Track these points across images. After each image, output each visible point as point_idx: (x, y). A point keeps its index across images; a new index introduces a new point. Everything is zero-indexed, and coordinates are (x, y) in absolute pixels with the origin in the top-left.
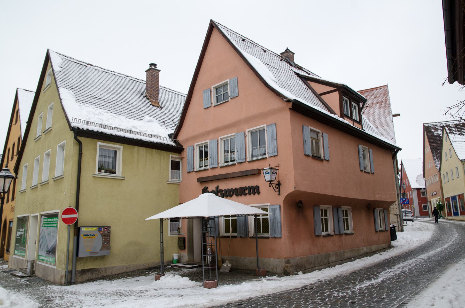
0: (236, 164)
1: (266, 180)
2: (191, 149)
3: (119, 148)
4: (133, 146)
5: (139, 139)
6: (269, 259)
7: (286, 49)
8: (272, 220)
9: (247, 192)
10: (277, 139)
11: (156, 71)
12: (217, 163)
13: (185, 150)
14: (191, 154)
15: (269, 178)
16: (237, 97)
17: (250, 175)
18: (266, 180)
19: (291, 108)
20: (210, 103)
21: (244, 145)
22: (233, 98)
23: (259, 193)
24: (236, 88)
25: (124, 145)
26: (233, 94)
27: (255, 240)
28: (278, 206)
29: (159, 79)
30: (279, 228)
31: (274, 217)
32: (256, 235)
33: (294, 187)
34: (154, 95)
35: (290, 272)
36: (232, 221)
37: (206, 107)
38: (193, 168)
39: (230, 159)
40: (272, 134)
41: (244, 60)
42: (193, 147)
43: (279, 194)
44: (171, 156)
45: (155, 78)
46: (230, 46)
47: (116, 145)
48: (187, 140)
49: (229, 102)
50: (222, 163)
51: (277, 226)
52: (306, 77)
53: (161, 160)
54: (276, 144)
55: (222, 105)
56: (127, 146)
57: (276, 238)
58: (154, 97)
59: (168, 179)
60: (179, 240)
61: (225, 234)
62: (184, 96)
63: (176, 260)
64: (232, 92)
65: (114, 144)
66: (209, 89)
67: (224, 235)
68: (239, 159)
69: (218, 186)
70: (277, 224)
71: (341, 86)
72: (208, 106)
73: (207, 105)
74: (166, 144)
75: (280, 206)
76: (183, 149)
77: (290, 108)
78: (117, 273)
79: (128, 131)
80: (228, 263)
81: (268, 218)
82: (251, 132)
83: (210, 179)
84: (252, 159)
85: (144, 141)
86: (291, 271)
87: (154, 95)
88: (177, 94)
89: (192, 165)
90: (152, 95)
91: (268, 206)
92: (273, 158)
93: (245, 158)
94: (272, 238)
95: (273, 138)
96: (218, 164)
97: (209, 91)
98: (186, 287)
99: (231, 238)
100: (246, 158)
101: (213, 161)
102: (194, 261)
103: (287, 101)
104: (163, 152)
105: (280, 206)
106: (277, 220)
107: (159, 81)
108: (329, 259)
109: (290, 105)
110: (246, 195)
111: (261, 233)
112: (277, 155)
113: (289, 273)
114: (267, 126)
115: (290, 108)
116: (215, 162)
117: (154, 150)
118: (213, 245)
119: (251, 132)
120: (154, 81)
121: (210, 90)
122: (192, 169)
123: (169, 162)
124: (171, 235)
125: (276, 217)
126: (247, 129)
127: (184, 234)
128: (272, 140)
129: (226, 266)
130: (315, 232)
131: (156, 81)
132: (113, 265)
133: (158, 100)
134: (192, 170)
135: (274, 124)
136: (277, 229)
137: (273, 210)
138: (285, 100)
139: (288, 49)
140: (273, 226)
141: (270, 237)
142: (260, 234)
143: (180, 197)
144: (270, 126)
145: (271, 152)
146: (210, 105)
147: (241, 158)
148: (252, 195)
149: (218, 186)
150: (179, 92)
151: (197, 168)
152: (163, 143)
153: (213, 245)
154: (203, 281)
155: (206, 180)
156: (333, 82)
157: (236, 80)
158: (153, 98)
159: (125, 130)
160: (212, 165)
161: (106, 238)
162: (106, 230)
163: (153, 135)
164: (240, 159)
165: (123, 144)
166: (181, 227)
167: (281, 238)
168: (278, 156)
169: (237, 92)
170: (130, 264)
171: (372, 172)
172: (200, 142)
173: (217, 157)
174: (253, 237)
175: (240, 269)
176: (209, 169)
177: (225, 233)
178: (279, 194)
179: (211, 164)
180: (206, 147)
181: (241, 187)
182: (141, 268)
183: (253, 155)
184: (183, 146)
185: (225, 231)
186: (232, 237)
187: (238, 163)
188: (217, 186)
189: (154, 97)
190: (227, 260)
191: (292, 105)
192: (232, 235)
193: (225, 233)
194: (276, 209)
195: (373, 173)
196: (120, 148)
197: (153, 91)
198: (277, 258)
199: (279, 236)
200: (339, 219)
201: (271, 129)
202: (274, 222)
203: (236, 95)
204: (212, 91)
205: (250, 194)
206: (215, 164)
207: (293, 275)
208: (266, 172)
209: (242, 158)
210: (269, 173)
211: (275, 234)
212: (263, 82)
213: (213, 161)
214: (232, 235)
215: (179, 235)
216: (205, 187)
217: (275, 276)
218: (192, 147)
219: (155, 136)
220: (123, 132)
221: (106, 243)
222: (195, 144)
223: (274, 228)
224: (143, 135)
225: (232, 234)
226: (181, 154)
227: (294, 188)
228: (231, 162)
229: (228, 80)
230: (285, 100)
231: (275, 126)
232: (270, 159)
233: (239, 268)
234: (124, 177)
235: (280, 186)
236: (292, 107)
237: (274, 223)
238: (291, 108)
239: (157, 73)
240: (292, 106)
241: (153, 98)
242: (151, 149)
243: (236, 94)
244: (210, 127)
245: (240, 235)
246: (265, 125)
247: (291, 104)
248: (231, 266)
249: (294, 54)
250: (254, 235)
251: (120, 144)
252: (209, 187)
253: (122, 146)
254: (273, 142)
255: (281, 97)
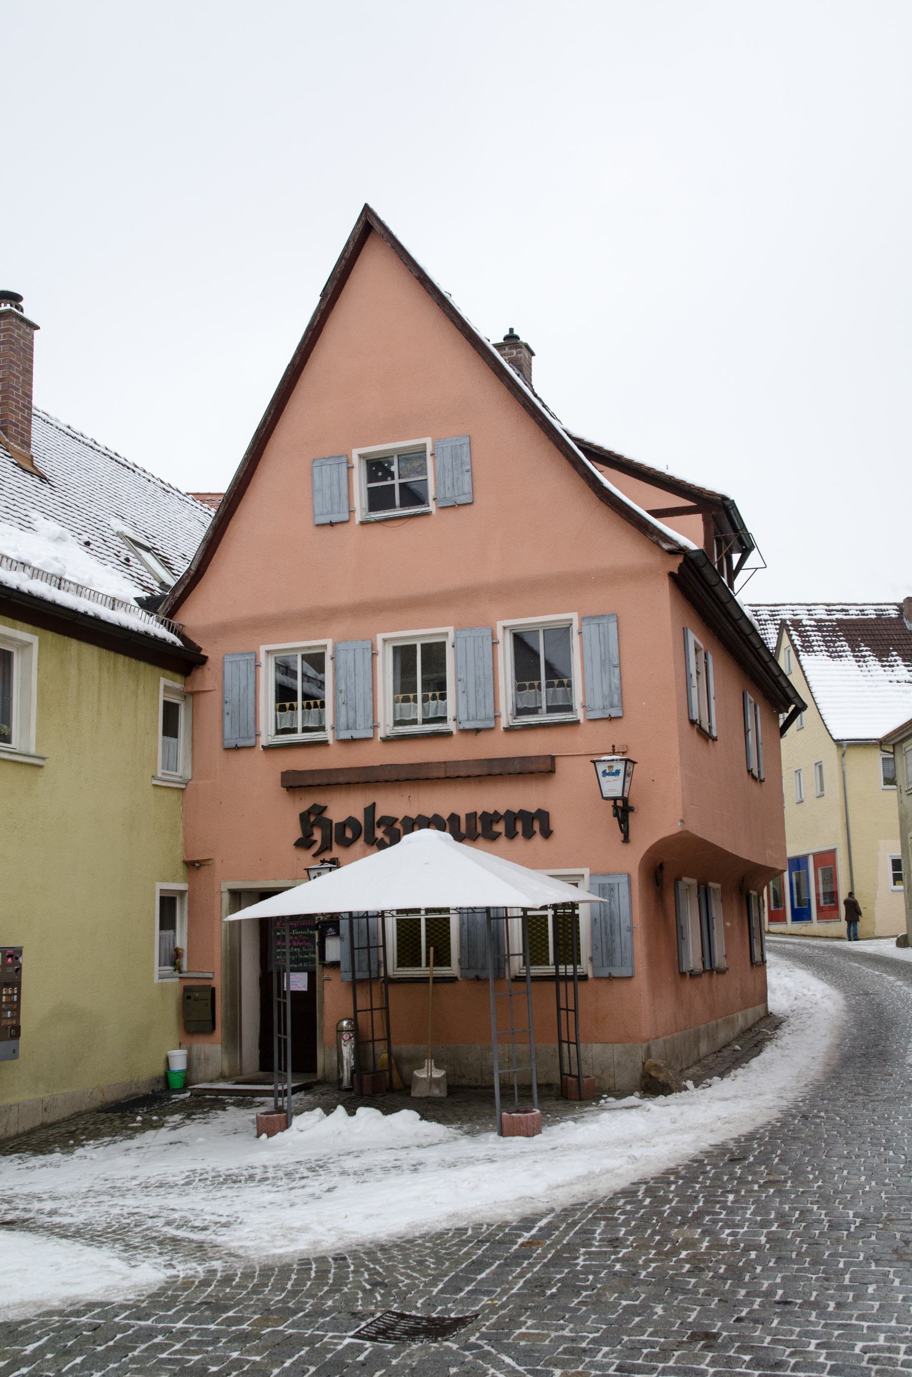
0: (455, 732)
1: (605, 796)
2: (243, 665)
3: (27, 642)
4: (66, 638)
5: (91, 613)
6: (587, 1047)
7: (507, 333)
8: (598, 920)
9: (500, 828)
10: (619, 666)
11: (24, 326)
12: (370, 724)
13: (209, 664)
14: (243, 683)
15: (615, 790)
16: (467, 508)
17: (519, 773)
18: (605, 796)
19: (676, 572)
20: (346, 510)
21: (491, 672)
22: (454, 506)
23: (547, 833)
24: (462, 472)
25: (43, 631)
26: (448, 495)
27: (552, 985)
28: (623, 880)
29: (32, 361)
30: (625, 947)
31: (608, 912)
32: (528, 970)
33: (682, 821)
34: (17, 426)
35: (670, 1082)
36: (427, 926)
37: (326, 520)
38: (252, 733)
39: (423, 715)
40: (602, 648)
41: (509, 388)
42: (254, 657)
43: (626, 840)
44: (163, 681)
45: (22, 353)
46: (451, 325)
47: (22, 630)
48: (226, 629)
49: (431, 518)
50: (386, 727)
51: (617, 940)
52: (594, 450)
53: (137, 697)
54: (616, 681)
55: (401, 522)
56: (50, 636)
57: (613, 978)
58: (19, 433)
59: (156, 769)
60: (189, 998)
61: (399, 969)
62: (67, 434)
63: (181, 1071)
64: (449, 483)
65: (16, 629)
66: (344, 460)
67: (395, 973)
68: (468, 717)
69: (374, 804)
70: (617, 934)
71: (717, 501)
72: (335, 518)
73: (332, 512)
74: (160, 639)
75: (629, 876)
76: (204, 660)
77: (671, 575)
78: (21, 1130)
79: (54, 579)
80: (433, 1068)
81: (547, 916)
82: (511, 630)
83: (341, 779)
84: (514, 721)
85: (105, 623)
86: (673, 1080)
87: (17, 426)
88: (48, 423)
89: (251, 723)
90: (12, 423)
91: (583, 876)
92: (604, 726)
93: (492, 715)
94: (597, 978)
95: (605, 662)
96: (375, 727)
97: (344, 468)
98: (424, 1142)
99: (434, 982)
100: (495, 717)
101: (351, 714)
102: (241, 1074)
103: (670, 552)
104: (142, 665)
105: (629, 876)
106: (617, 920)
107: (32, 367)
108: (698, 1050)
109: (674, 564)
110: (493, 837)
111: (548, 964)
112: (620, 718)
113: (668, 1085)
114: (582, 619)
115: (671, 575)
116: (360, 721)
117: (121, 658)
118: (372, 1013)
119: (511, 630)
120: (19, 366)
121: (348, 462)
122: (249, 738)
123: (158, 702)
124: (161, 981)
125: (616, 911)
126: (503, 619)
127: (210, 975)
128: (603, 664)
129: (424, 1076)
130: (679, 963)
131: (24, 368)
132: (10, 1100)
133: (29, 445)
134: (251, 742)
135: (612, 615)
136: (618, 950)
137: (604, 889)
138: (666, 546)
139: (515, 333)
140: (604, 940)
141: (590, 975)
142: (547, 967)
143: (185, 838)
144: (597, 621)
145: (598, 702)
146: (345, 517)
147: (479, 714)
148: (520, 839)
149: (374, 804)
150: (47, 415)
151: (267, 735)
152: (152, 634)
153: (372, 1013)
154: (492, 1116)
155: (325, 781)
156: (688, 482)
157: (466, 449)
158: (14, 437)
159: (45, 575)
160: (347, 729)
161: (10, 992)
162: (10, 960)
163: (119, 601)
164: (475, 719)
165: (38, 630)
166: (185, 947)
167: (630, 978)
168: (623, 720)
169: (467, 488)
170: (55, 1093)
171: (762, 777)
172: (286, 641)
173: (370, 702)
174: (518, 979)
175: (470, 1087)
176: (331, 742)
177: (398, 966)
178: (626, 840)
179: (343, 727)
180: (316, 660)
181: (476, 813)
182: (83, 1108)
183: (517, 709)
184: (200, 649)
185: (399, 962)
186: (434, 978)
187: (464, 731)
188: (368, 804)
189: (19, 433)
190: (425, 1058)
191: (680, 564)
192: (434, 972)
193: (398, 966)
194: (616, 885)
195: (762, 781)
196: (31, 644)
197: (16, 407)
198: (619, 1043)
199: (625, 972)
200: (710, 920)
201: (601, 631)
202: (606, 928)
203: (463, 497)
204: (353, 467)
205: (511, 835)
206: (362, 727)
207: (680, 1091)
208: (607, 769)
209: (483, 716)
210: (617, 772)
211: (611, 964)
212: (586, 475)
213: (351, 714)
214: (434, 972)
215: (180, 978)
216: (315, 805)
217: (633, 1097)
218: (248, 657)
219: (123, 603)
220: (47, 585)
221: (9, 1012)
222: (263, 649)
223: (607, 945)
224: (92, 597)
225: (434, 968)
226: (189, 678)
227: (679, 824)
228: (424, 726)
229: (428, 441)
230: (666, 546)
231: (615, 624)
232: (591, 726)
233: (464, 1082)
234: (44, 759)
235: (631, 815)
236: (679, 569)
237: (609, 931)
238: (676, 572)
239: (28, 334)
240: (680, 568)
241: (14, 437)
242: (112, 653)
243: (464, 494)
244: (341, 596)
245: (472, 974)
246: (574, 616)
247: (679, 560)
248: (447, 1076)
249: (533, 354)
250: (522, 971)
251: (30, 627)
252: (329, 807)
253: (36, 634)
254: (607, 673)
255: (652, 534)
